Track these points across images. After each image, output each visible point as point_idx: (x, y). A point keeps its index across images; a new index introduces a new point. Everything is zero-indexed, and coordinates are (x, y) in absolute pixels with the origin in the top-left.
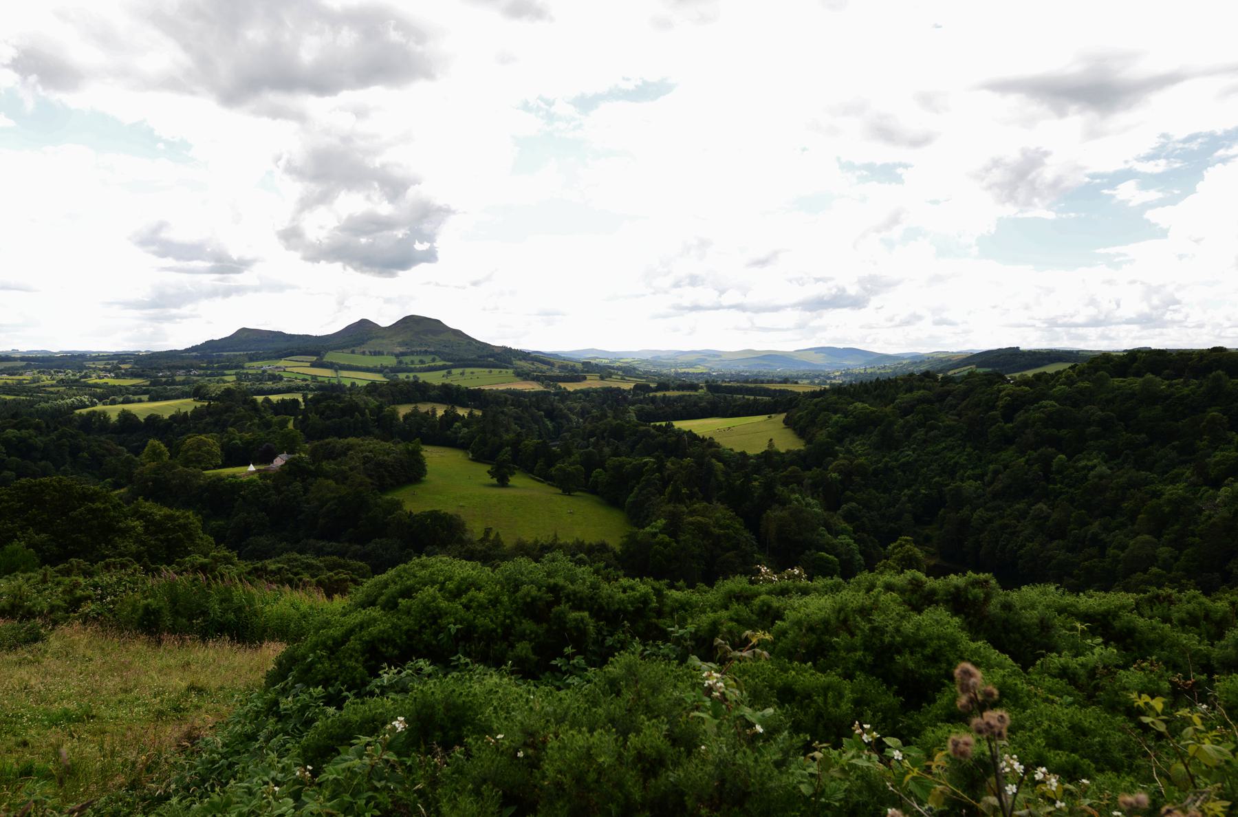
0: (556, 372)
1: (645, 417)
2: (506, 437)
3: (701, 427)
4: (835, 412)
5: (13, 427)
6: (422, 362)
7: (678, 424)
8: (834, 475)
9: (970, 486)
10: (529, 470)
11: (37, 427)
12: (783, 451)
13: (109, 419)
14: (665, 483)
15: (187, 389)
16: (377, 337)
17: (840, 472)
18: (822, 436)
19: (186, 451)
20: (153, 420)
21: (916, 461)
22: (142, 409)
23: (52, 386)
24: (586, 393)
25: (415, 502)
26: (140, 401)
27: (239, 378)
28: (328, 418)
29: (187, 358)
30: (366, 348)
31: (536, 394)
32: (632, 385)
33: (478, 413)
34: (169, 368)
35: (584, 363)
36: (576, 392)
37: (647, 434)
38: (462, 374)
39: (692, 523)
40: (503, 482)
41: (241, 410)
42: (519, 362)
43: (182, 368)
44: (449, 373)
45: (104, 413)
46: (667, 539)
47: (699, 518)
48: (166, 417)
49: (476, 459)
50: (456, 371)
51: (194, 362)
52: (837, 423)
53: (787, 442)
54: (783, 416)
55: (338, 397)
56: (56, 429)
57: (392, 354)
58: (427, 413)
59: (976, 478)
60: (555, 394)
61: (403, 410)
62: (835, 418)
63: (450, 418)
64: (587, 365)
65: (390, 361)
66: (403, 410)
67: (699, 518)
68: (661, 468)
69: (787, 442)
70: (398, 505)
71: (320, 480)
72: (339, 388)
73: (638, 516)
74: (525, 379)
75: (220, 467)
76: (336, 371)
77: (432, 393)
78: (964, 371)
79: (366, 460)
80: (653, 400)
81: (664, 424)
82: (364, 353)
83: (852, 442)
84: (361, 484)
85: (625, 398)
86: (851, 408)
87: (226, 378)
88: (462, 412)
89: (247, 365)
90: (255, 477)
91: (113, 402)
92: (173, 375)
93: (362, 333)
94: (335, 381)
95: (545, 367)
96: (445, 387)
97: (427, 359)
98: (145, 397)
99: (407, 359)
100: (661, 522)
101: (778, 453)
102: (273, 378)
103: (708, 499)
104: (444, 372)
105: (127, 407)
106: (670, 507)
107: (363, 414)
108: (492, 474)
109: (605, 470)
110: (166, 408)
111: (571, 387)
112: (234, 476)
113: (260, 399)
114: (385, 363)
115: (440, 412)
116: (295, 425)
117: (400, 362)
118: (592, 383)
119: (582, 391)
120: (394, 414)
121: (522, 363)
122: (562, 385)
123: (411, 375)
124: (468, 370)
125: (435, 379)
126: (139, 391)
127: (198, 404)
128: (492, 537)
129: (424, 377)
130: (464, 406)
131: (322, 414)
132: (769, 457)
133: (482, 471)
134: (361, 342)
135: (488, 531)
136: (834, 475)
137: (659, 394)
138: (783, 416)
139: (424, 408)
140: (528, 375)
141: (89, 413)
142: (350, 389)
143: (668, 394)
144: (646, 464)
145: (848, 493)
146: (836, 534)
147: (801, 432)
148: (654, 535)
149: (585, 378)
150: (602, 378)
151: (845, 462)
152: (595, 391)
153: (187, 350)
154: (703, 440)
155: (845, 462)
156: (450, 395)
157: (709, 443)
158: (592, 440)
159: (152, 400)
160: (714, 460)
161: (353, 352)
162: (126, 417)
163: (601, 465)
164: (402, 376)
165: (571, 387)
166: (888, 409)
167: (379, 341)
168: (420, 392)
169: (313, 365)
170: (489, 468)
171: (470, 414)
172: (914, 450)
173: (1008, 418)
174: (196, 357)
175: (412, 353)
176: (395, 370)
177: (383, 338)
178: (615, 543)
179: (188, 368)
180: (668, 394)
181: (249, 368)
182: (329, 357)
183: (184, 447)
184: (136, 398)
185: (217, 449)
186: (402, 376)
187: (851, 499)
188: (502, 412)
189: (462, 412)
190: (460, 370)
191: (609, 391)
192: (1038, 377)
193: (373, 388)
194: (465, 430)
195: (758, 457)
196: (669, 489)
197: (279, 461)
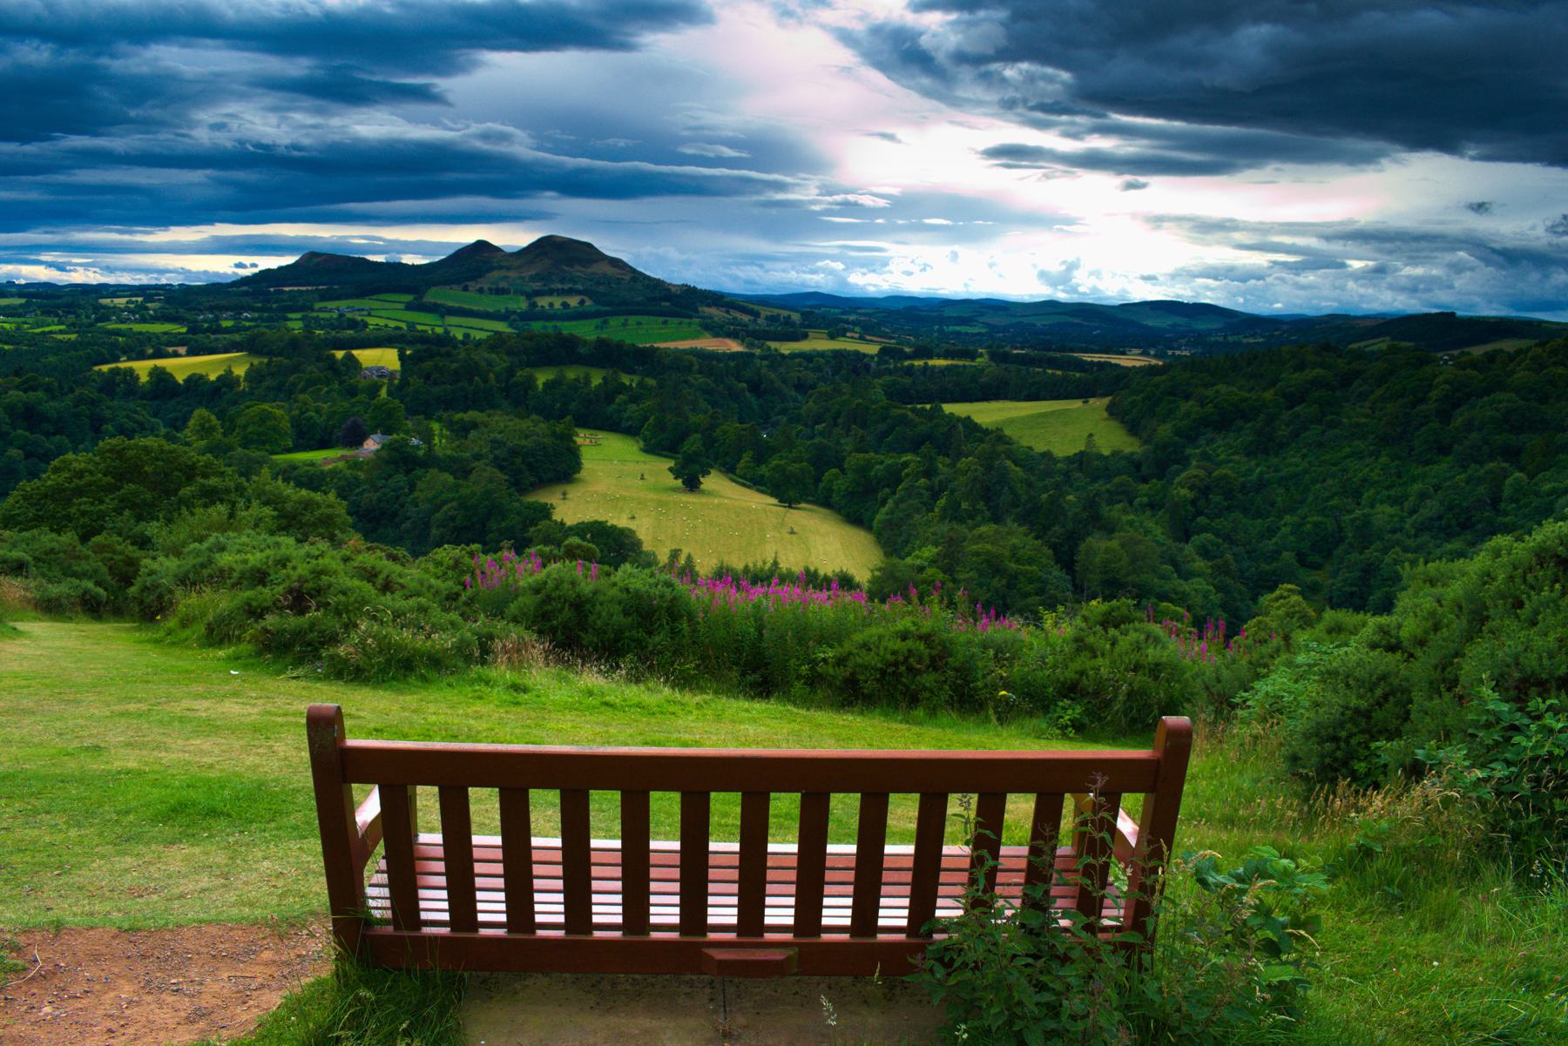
1: (901, 395)
2: (694, 419)
3: (986, 414)
4: (1187, 397)
5: (17, 388)
6: (565, 305)
7: (948, 408)
8: (1184, 492)
9: (1383, 513)
10: (729, 470)
11: (48, 389)
12: (1106, 452)
13: (138, 378)
14: (935, 496)
15: (237, 337)
16: (501, 268)
17: (1191, 488)
18: (1165, 431)
19: (245, 427)
20: (195, 381)
21: (1306, 471)
22: (181, 366)
23: (61, 332)
24: (808, 357)
25: (571, 508)
26: (176, 355)
27: (309, 325)
28: (436, 383)
29: (236, 294)
30: (484, 283)
31: (733, 356)
33: (651, 382)
34: (211, 309)
36: (793, 356)
37: (903, 420)
38: (625, 324)
39: (978, 554)
40: (692, 485)
41: (313, 369)
42: (707, 310)
43: (228, 309)
44: (605, 322)
45: (131, 370)
46: (941, 576)
47: (989, 547)
48: (213, 377)
49: (650, 449)
50: (614, 322)
51: (246, 300)
52: (1187, 415)
53: (1112, 440)
54: (1106, 400)
55: (448, 355)
56: (72, 391)
57: (523, 293)
58: (577, 380)
59: (1397, 501)
60: (763, 358)
61: (542, 378)
62: (1184, 406)
63: (611, 391)
65: (522, 304)
66: (542, 378)
67: (989, 547)
68: (929, 473)
69: (1112, 440)
70: (546, 511)
71: (434, 471)
72: (445, 341)
73: (892, 541)
74: (716, 335)
75: (289, 451)
76: (443, 316)
77: (582, 351)
78: (1381, 344)
79: (496, 444)
80: (909, 371)
81: (928, 407)
82: (481, 291)
83: (1210, 441)
84: (491, 481)
85: (867, 368)
86: (1210, 392)
87: (290, 324)
88: (626, 379)
89: (318, 305)
90: (341, 465)
91: (142, 356)
92: (217, 319)
94: (439, 330)
95: (746, 318)
96: (602, 344)
97: (573, 301)
98: (182, 350)
99: (543, 302)
100: (930, 551)
101: (1100, 457)
102: (353, 324)
103: (997, 519)
104: (597, 321)
105: (161, 363)
106: (945, 527)
107: (486, 380)
108: (677, 473)
109: (843, 470)
110: (209, 365)
111: (786, 348)
112: (312, 464)
113: (340, 354)
114: (512, 306)
115: (596, 380)
116: (389, 393)
118: (819, 344)
119: (802, 355)
120: (530, 383)
121: (713, 311)
122: (773, 345)
123: (550, 324)
124: (632, 320)
125: (586, 331)
126: (179, 341)
127: (256, 361)
128: (682, 561)
129: (568, 328)
130: (631, 372)
131: (427, 377)
132: (1081, 461)
133: (660, 469)
134: (477, 274)
135: (675, 554)
136: (1184, 492)
137: (918, 363)
138: (1106, 400)
139: (571, 374)
140: (721, 327)
141: (111, 370)
142: (463, 343)
143: (931, 363)
144: (905, 465)
145: (1201, 520)
146: (1186, 576)
147: (1133, 428)
148: (921, 569)
149: (805, 336)
150: (832, 337)
151: (1202, 473)
152: (822, 354)
154: (987, 432)
155: (1202, 473)
156: (608, 355)
157: (996, 436)
158: (819, 427)
159: (191, 353)
160: (1009, 463)
161: (466, 289)
162: (160, 376)
163: (839, 463)
164: (537, 326)
165: (786, 348)
166: (1268, 395)
167: (503, 273)
168: (563, 351)
169: (410, 307)
170: (672, 464)
171: (641, 385)
172: (1304, 456)
173: (1445, 416)
174: (246, 294)
175: (551, 293)
176: (527, 317)
177: (509, 269)
178: (862, 576)
179: (238, 310)
180: (931, 363)
181: (320, 310)
182: (434, 296)
183: (241, 421)
184: (170, 350)
185: (286, 424)
186: (537, 326)
187: (1204, 529)
188: (686, 382)
189: (626, 379)
190: (621, 319)
191: (838, 354)
192: (1491, 357)
193: (497, 342)
194: (634, 407)
195: (1069, 460)
196: (942, 502)
197: (372, 445)
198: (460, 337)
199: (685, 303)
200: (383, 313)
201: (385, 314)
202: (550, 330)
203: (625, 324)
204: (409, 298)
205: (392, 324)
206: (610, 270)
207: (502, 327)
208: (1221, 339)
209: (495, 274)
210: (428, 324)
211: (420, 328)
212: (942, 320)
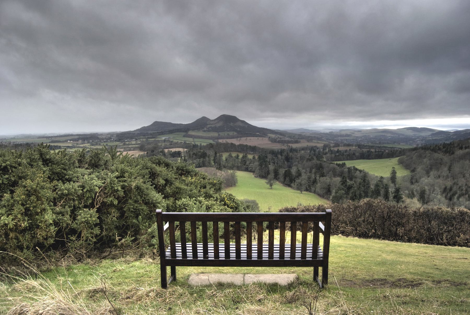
0: (287, 139)
6: (228, 134)
16: (210, 124)
30: (205, 129)
32: (322, 145)
35: (299, 135)
38: (246, 140)
64: (300, 135)
82: (204, 131)
93: (202, 124)
94: (193, 143)
96: (240, 145)
117: (219, 135)
118: (304, 144)
122: (290, 145)
124: (249, 138)
153: (135, 131)
156: (244, 149)
169: (184, 136)
190: (245, 138)
198: (199, 145)
199: (263, 132)
200: (177, 138)
201: (178, 138)
202: (224, 142)
203: (246, 140)
204: (183, 134)
205: (180, 141)
206: (241, 124)
207: (211, 141)
208: (431, 139)
209: (209, 126)
210: (190, 140)
211: (187, 142)
212: (341, 136)
